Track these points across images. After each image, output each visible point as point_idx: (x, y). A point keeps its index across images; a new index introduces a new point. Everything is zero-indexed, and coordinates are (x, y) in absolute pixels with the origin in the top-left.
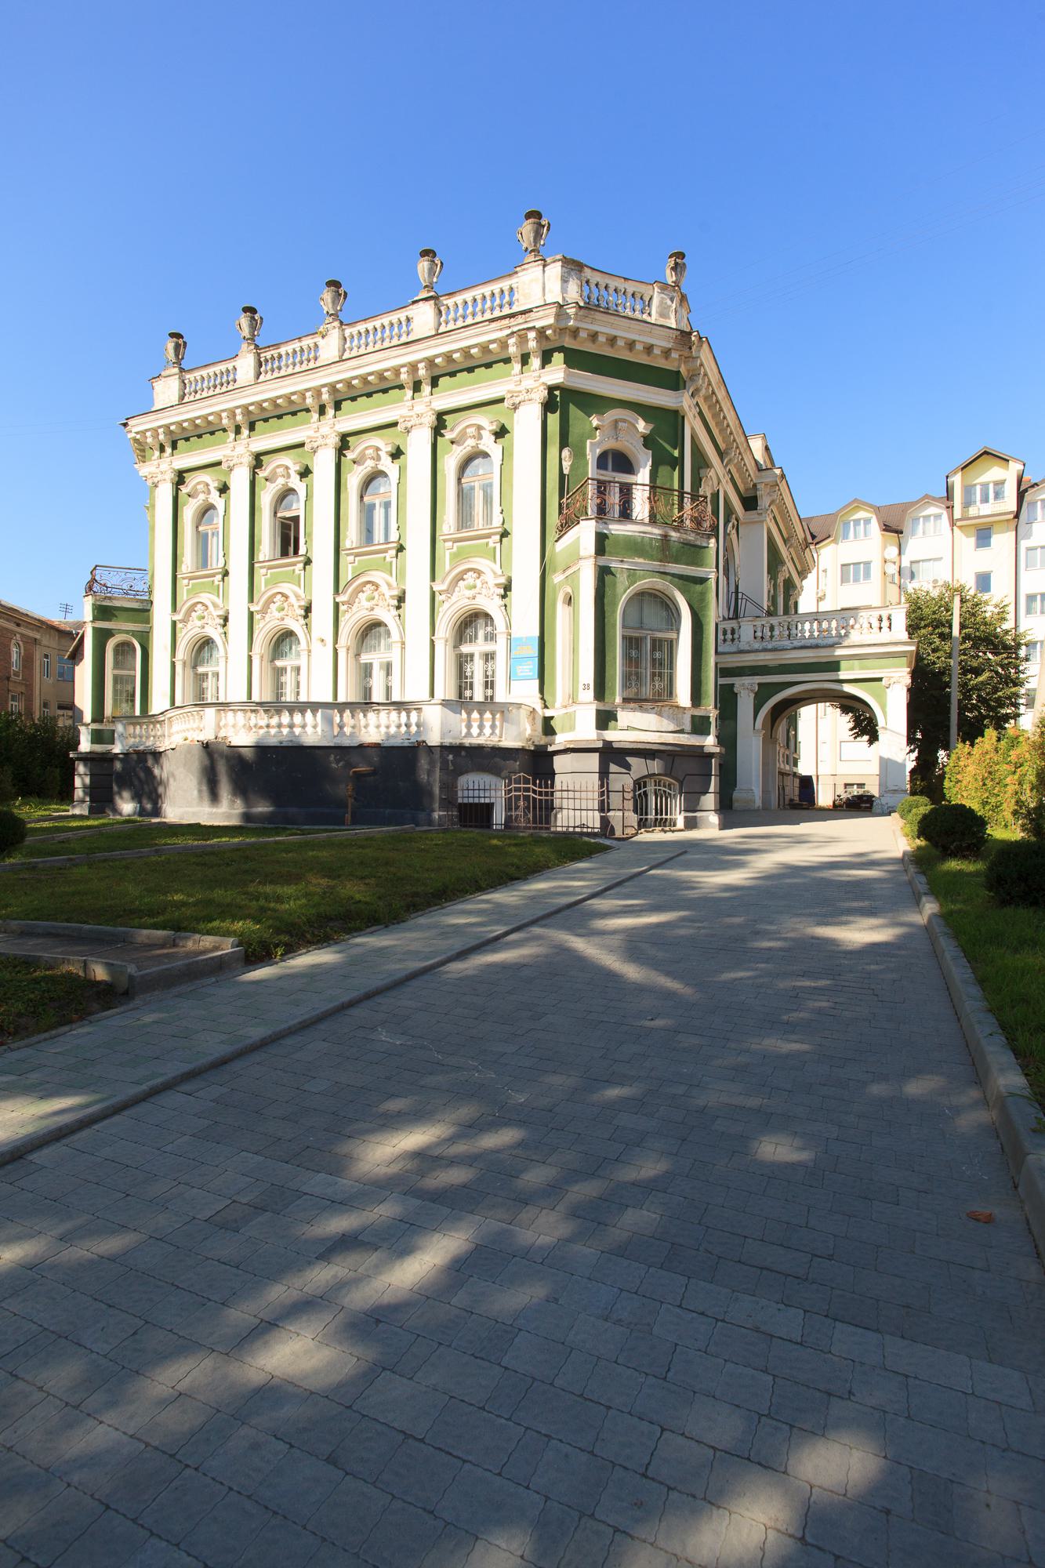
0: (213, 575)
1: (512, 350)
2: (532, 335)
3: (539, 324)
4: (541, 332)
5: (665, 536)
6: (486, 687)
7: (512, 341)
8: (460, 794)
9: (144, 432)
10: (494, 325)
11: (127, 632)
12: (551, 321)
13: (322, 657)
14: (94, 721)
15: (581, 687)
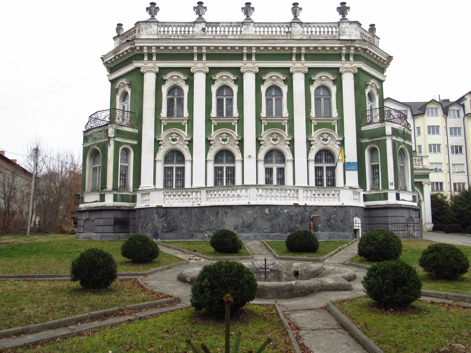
0: (183, 120)
1: (344, 51)
2: (352, 48)
3: (357, 46)
4: (356, 49)
5: (404, 129)
6: (328, 181)
7: (344, 49)
8: (355, 224)
9: (142, 48)
10: (338, 42)
11: (128, 144)
12: (362, 46)
13: (250, 165)
14: (114, 189)
15: (389, 184)
